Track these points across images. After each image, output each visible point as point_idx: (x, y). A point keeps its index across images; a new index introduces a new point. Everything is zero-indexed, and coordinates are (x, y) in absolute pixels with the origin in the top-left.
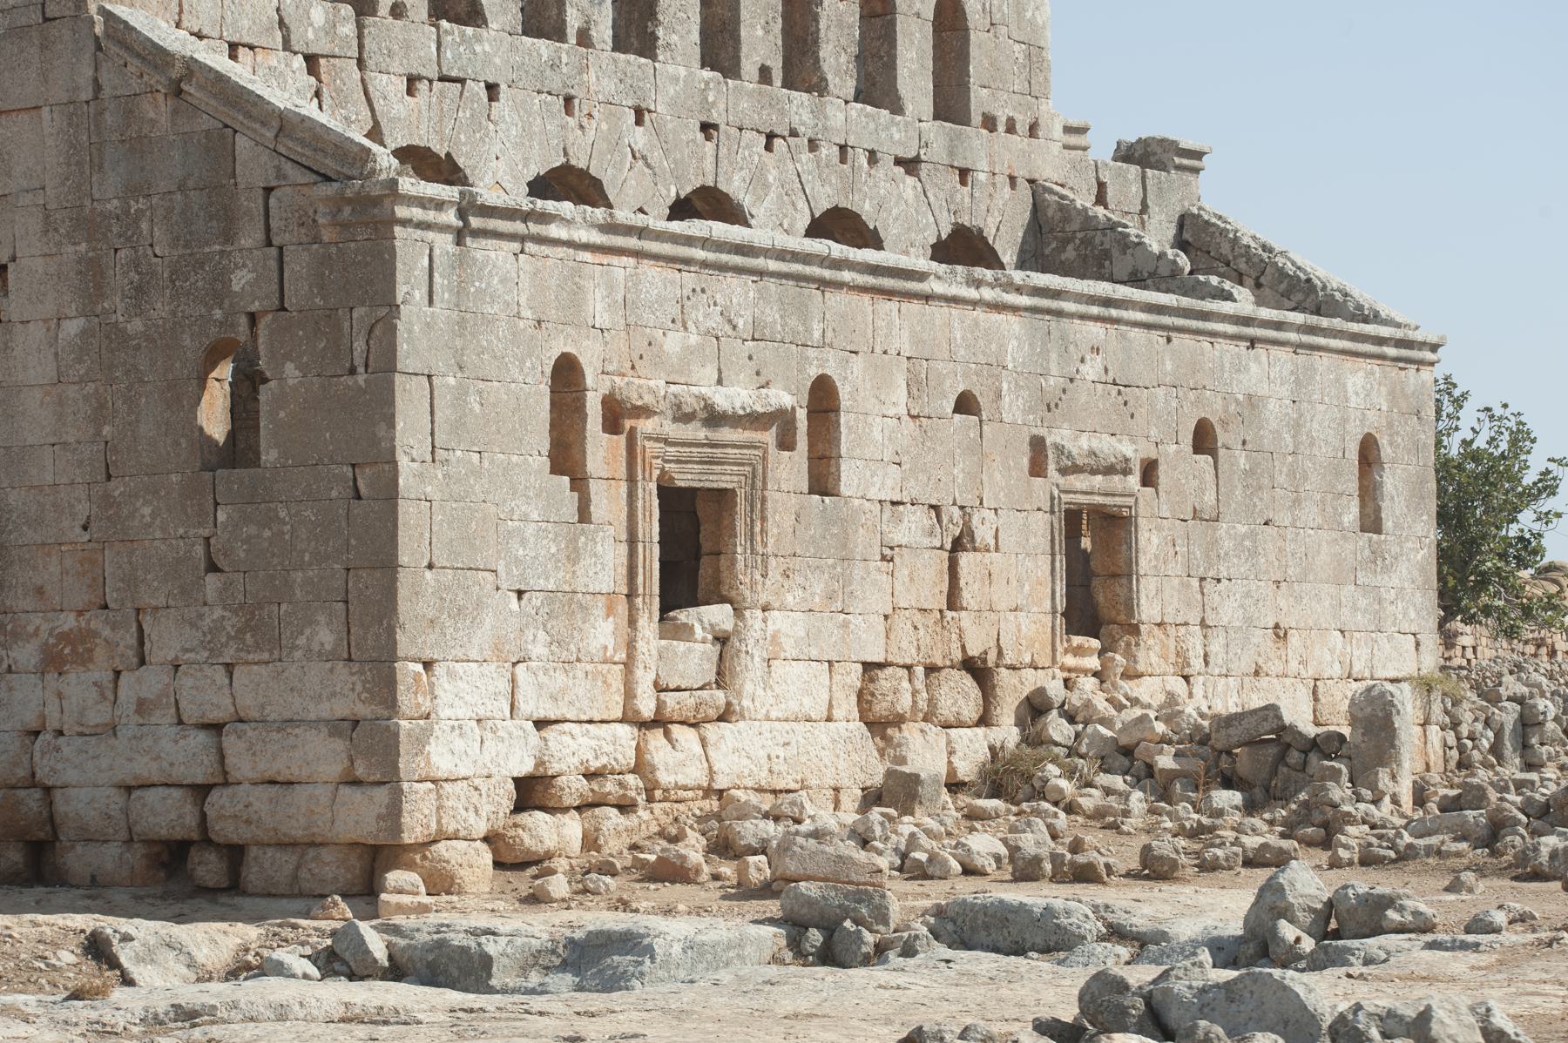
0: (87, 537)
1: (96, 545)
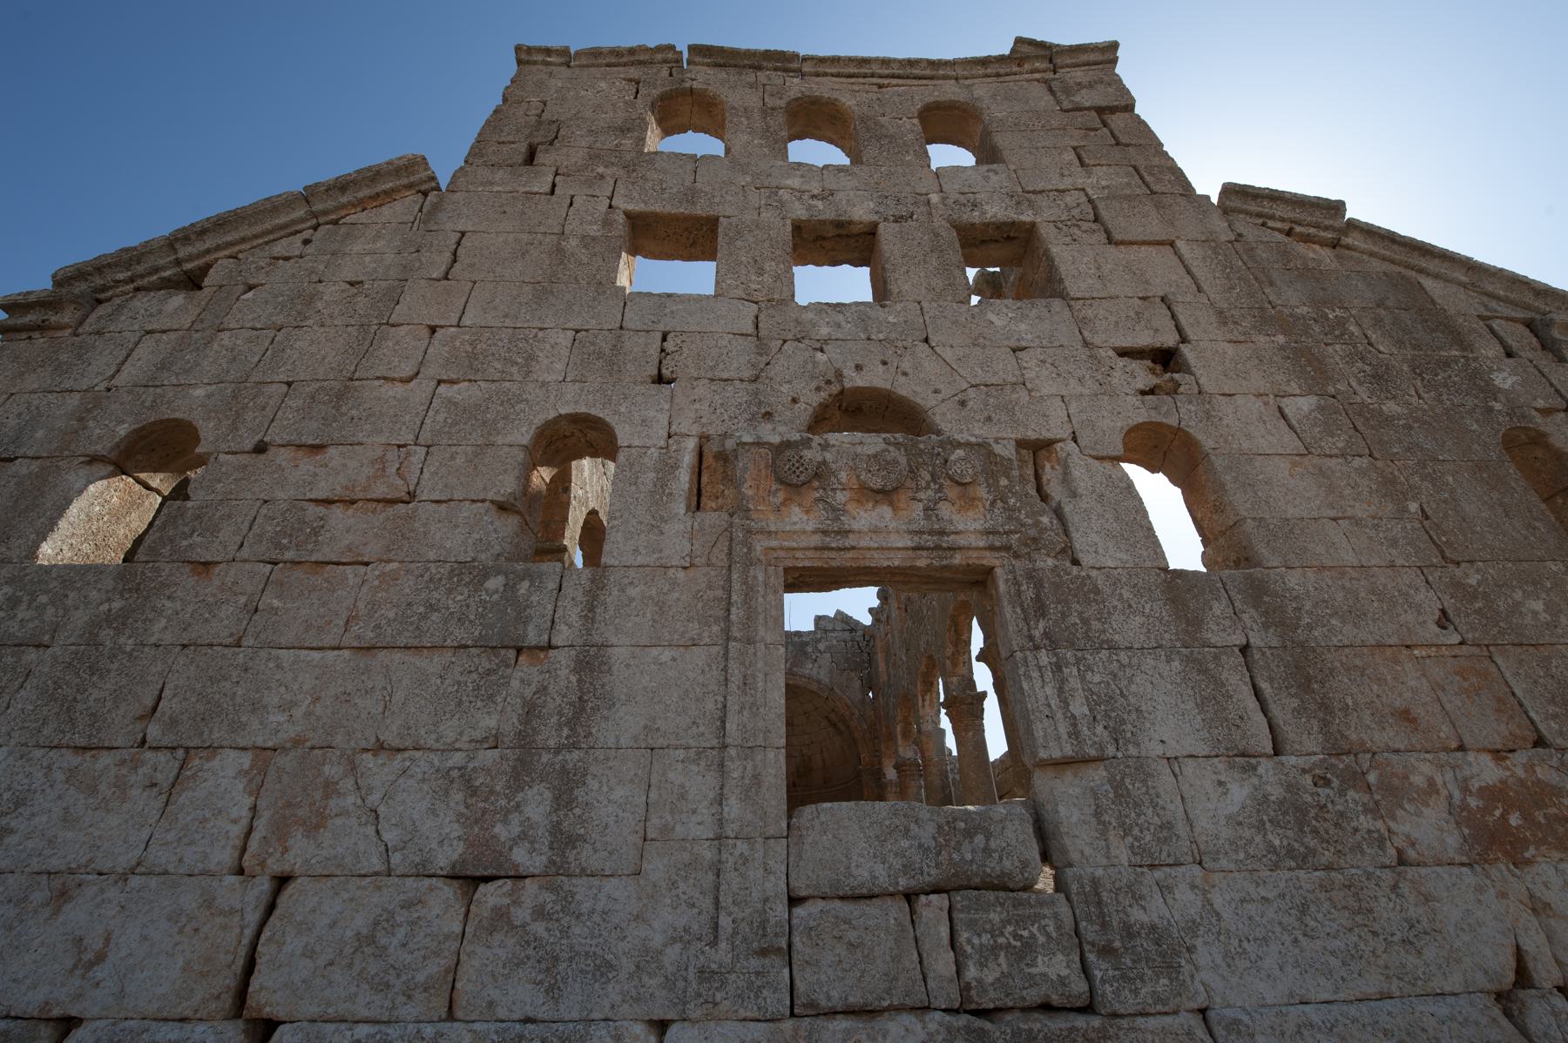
0: (1456, 639)
1: (1476, 650)
